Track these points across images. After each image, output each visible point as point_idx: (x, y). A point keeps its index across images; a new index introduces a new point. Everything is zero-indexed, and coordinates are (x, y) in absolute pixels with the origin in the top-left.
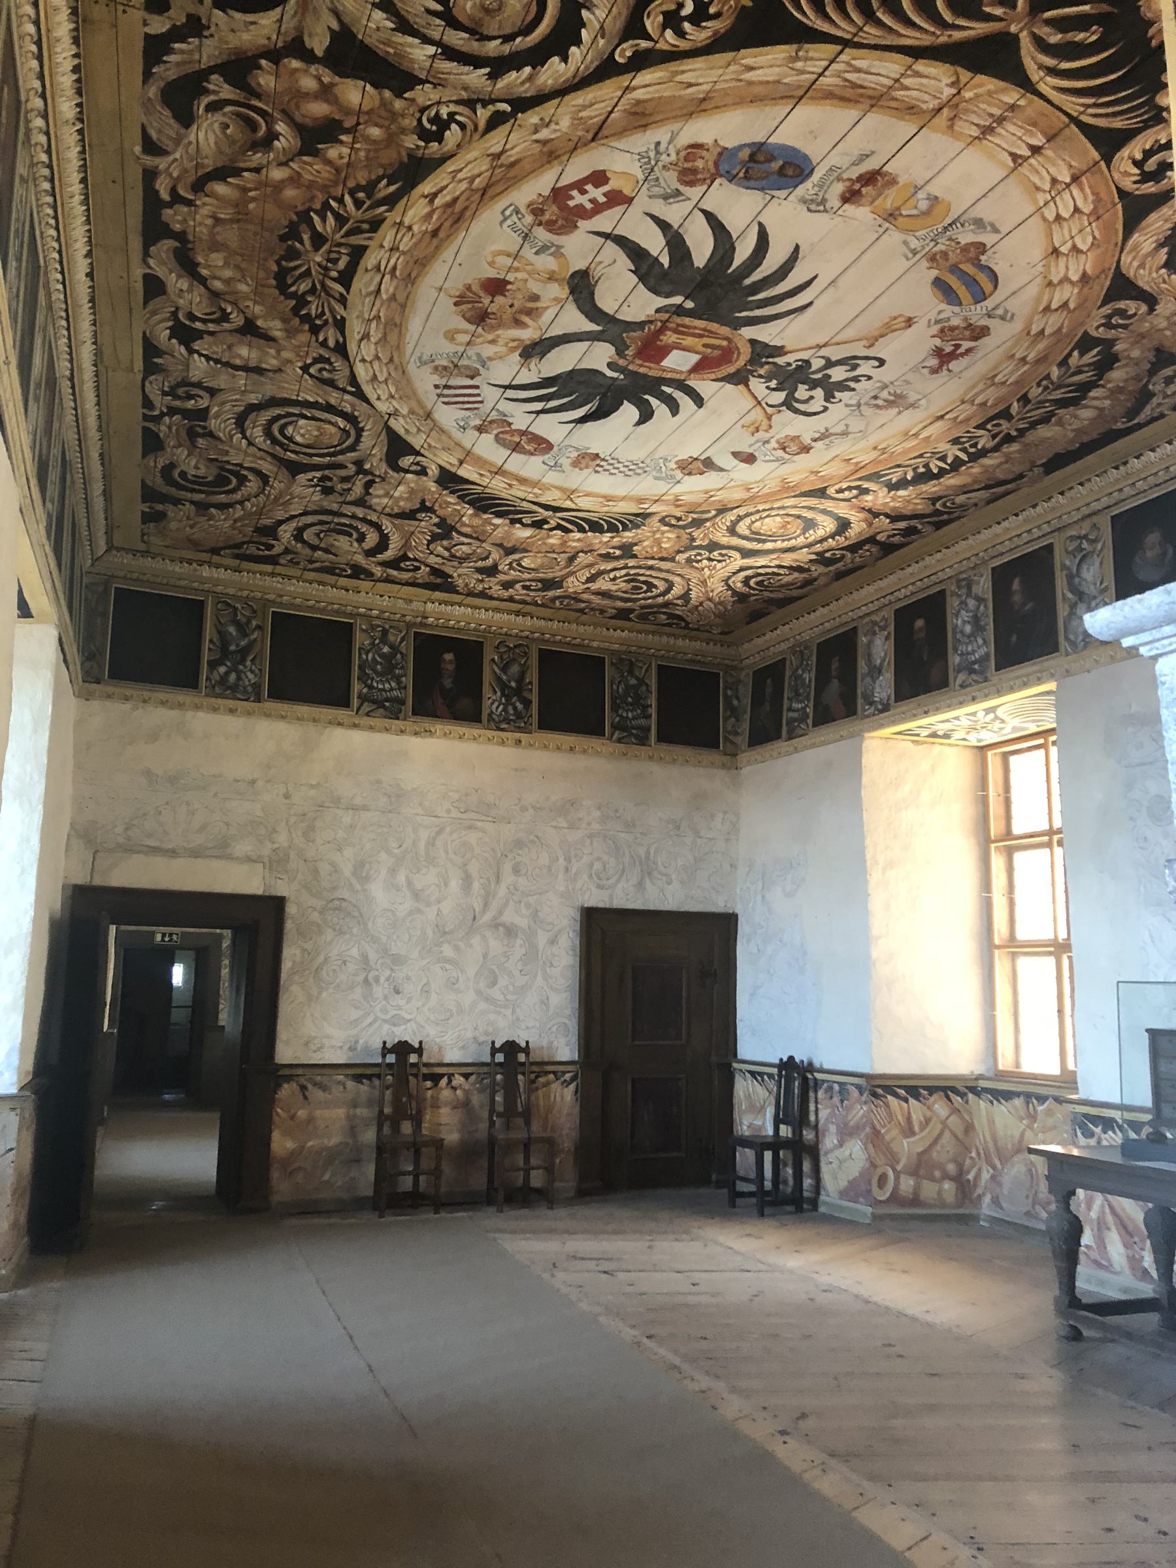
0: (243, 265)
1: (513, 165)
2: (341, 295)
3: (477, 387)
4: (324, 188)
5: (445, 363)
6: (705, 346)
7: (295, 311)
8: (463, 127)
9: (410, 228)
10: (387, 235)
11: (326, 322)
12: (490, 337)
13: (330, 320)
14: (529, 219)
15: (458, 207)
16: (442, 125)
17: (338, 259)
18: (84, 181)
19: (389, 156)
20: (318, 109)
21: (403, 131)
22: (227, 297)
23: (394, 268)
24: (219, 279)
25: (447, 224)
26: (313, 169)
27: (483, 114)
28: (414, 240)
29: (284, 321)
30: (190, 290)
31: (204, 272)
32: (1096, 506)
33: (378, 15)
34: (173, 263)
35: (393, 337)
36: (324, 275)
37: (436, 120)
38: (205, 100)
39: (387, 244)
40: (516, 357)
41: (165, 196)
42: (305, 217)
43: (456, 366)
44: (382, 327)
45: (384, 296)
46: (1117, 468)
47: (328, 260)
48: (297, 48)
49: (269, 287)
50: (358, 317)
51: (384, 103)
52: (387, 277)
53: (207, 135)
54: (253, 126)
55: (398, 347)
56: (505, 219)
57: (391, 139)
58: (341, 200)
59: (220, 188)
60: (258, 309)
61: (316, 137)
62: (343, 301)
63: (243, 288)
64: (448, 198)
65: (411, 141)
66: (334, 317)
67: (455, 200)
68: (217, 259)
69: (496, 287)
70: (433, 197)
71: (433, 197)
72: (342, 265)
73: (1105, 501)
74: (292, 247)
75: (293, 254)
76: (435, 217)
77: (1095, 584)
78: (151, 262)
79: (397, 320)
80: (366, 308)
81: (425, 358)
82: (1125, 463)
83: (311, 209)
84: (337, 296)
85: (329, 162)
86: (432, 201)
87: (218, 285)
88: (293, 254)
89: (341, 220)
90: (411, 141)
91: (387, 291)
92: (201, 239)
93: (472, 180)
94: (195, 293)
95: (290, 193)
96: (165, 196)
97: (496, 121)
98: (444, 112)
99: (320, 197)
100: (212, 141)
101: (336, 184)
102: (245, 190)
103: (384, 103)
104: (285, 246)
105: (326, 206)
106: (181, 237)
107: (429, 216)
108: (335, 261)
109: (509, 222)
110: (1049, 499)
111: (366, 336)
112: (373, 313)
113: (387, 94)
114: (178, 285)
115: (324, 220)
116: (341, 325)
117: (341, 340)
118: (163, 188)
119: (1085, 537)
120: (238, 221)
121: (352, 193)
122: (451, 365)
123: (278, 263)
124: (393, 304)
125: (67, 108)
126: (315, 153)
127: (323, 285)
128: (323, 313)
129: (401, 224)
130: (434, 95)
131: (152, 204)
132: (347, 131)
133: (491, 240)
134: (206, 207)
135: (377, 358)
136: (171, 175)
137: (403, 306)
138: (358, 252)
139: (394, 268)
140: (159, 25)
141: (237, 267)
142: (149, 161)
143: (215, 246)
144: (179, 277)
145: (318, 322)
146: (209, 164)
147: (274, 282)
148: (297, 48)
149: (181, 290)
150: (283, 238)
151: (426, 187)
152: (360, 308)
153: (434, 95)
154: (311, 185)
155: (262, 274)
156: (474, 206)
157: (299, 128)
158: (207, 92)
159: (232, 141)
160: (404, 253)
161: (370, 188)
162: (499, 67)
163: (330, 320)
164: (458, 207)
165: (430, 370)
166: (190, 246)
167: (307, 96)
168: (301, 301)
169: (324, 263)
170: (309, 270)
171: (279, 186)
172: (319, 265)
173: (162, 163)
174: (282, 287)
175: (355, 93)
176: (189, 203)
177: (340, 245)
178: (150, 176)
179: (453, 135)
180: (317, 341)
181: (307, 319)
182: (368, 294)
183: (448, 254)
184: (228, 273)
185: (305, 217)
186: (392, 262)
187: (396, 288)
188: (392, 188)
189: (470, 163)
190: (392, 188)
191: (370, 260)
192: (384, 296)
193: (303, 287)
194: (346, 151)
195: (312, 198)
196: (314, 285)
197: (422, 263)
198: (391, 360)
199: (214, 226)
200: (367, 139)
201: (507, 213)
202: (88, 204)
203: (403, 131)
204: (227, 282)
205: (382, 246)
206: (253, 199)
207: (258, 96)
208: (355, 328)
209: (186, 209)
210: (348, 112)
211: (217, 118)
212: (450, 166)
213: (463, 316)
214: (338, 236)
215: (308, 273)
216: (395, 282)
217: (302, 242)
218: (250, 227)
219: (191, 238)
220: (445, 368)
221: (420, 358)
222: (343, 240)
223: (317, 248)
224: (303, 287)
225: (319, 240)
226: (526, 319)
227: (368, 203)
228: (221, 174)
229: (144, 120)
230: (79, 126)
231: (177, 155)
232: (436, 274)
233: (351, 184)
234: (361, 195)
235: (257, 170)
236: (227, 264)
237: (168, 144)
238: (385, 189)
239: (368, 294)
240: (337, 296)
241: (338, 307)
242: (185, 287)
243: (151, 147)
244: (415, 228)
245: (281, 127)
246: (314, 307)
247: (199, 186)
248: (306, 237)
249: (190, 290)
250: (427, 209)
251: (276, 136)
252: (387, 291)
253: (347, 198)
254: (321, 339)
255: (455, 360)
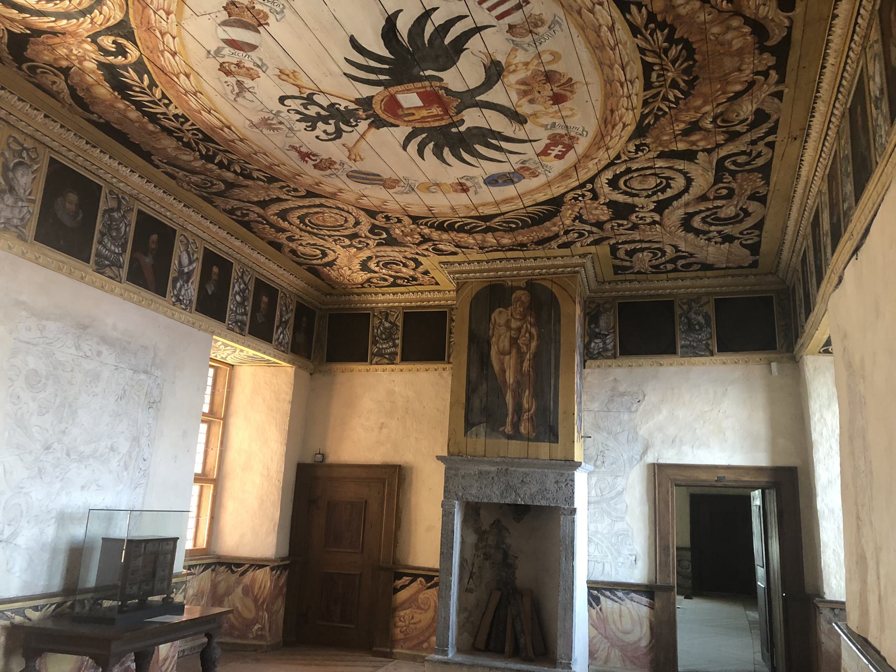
0: (719, 47)
1: (599, 148)
2: (645, 55)
3: (500, 17)
4: (681, 111)
5: (541, 30)
6: (414, 114)
7: (673, 30)
8: (630, 152)
9: (627, 109)
10: (637, 101)
11: (646, 28)
12: (532, 67)
13: (644, 31)
14: (573, 134)
15: (610, 127)
16: (638, 148)
17: (658, 77)
18: (823, 67)
19: (655, 133)
20: (694, 138)
21: (653, 142)
22: (726, 15)
23: (622, 86)
24: (735, 29)
25: (609, 118)
26: (689, 117)
27: (624, 158)
28: (621, 104)
29: (678, 16)
30: (757, 7)
31: (747, 29)
32: (46, 140)
33: (681, 168)
34: (770, 26)
35: (593, 36)
36: (662, 64)
37: (642, 151)
38: (749, 121)
39: (634, 98)
40: (501, 58)
41: (773, 73)
42: (686, 94)
43: (531, 32)
44: (606, 43)
45: (617, 66)
46: (87, 143)
47: (663, 75)
48: (709, 151)
49: (697, 42)
50: (626, 43)
51: (667, 147)
52: (623, 79)
53: (747, 109)
54: (723, 121)
55: (582, 29)
56: (583, 130)
57: (657, 138)
58: (669, 108)
59: (738, 88)
60: (701, 17)
61: (694, 127)
62: (642, 51)
63: (715, 30)
64: (617, 128)
65: (648, 141)
66: (642, 34)
67: (613, 128)
68: (737, 44)
69: (557, 99)
70: (625, 126)
71: (625, 126)
72: (654, 76)
73: (55, 145)
74: (688, 76)
75: (686, 71)
76: (617, 118)
77: (25, 191)
78: (787, 23)
79: (598, 51)
80: (624, 52)
81: (557, 28)
82: (94, 147)
83: (684, 99)
84: (647, 53)
85: (684, 122)
86: (624, 124)
87: (736, 22)
88: (686, 71)
89: (665, 99)
90: (648, 141)
91: (618, 71)
92: (749, 53)
93: (612, 138)
94: (753, 7)
95: (699, 102)
96: (773, 73)
97: (618, 157)
98: (640, 153)
99: (681, 106)
100: (744, 107)
101: (675, 115)
102: (724, 93)
103: (667, 147)
104: (694, 74)
105: (677, 103)
106: (763, 49)
107: (621, 119)
108: (659, 76)
109: (581, 129)
110: (35, 109)
111: (612, 29)
112: (617, 51)
113: (666, 150)
114: (767, 8)
115: (675, 96)
116: (635, 30)
117: (628, 16)
118: (774, 75)
119: (27, 150)
120: (726, 75)
121: (666, 113)
122: (535, 30)
123: (695, 61)
124: (608, 62)
125: (821, 107)
126: (690, 123)
127: (660, 58)
128: (651, 35)
129: (633, 109)
130: (648, 156)
131: (781, 67)
132: (678, 135)
133: (583, 115)
134: (747, 75)
135: (591, 11)
136: (768, 85)
137: (601, 64)
138: (648, 85)
139: (622, 86)
140: (770, 138)
141: (722, 45)
142: (780, 88)
143: (740, 52)
144: (766, 17)
145: (652, 26)
146: (745, 97)
147: (694, 46)
148: (709, 151)
149: (765, 5)
150: (696, 78)
151: (630, 129)
152: (628, 51)
153: (648, 156)
154: (688, 110)
155: (704, 48)
156: (603, 129)
157: (701, 129)
158: (747, 125)
159: (733, 111)
160: (623, 96)
161: (657, 118)
162: (628, 171)
163: (644, 31)
164: (610, 127)
165: (544, 17)
166: (757, 45)
167: (701, 140)
168: (670, 39)
169: (665, 72)
170: (674, 66)
171: (705, 103)
172: (667, 70)
173: (774, 89)
174: (688, 46)
175: (681, 146)
176: (758, 73)
177: (661, 86)
178: (781, 80)
179: (632, 148)
180: (646, 6)
181: (662, 26)
182: (628, 63)
183: (598, 105)
184: (729, 36)
185: (686, 94)
186: (626, 90)
187: (613, 75)
188: (647, 121)
189: (618, 140)
190: (647, 121)
191: (639, 85)
192: (617, 66)
193: (673, 52)
194: (676, 128)
195: (685, 104)
196: (667, 57)
197: (608, 96)
198: (579, 13)
199: (741, 65)
200: (669, 134)
201: (585, 133)
202: (825, 53)
203: (653, 142)
204: (729, 28)
205: (637, 95)
206: (718, 91)
207: (723, 132)
208: (623, 32)
209: (759, 69)
210: (681, 140)
211: (741, 118)
212: (625, 138)
213: (560, 74)
214: (664, 90)
215: (674, 62)
216: (616, 78)
217: (684, 81)
218: (717, 75)
219: (756, 51)
220: (536, 26)
221: (560, 25)
222: (659, 89)
223: (673, 80)
224: (673, 52)
225: (674, 85)
226: (523, 87)
227: (655, 111)
228: (738, 95)
229: (781, 105)
230: (818, 94)
231: (763, 95)
232: (596, 91)
233: (668, 116)
234: (660, 113)
235: (718, 105)
236: (730, 43)
237: (769, 99)
238: (650, 119)
239: (628, 63)
240: (647, 53)
241: (643, 44)
242: (762, 7)
243: (779, 95)
244: (624, 110)
245: (710, 126)
246: (660, 38)
247: (751, 84)
248: (682, 84)
249: (757, 7)
250: (624, 120)
251: (711, 122)
252: (618, 71)
253: (667, 110)
254: (644, 10)
255: (536, 37)
